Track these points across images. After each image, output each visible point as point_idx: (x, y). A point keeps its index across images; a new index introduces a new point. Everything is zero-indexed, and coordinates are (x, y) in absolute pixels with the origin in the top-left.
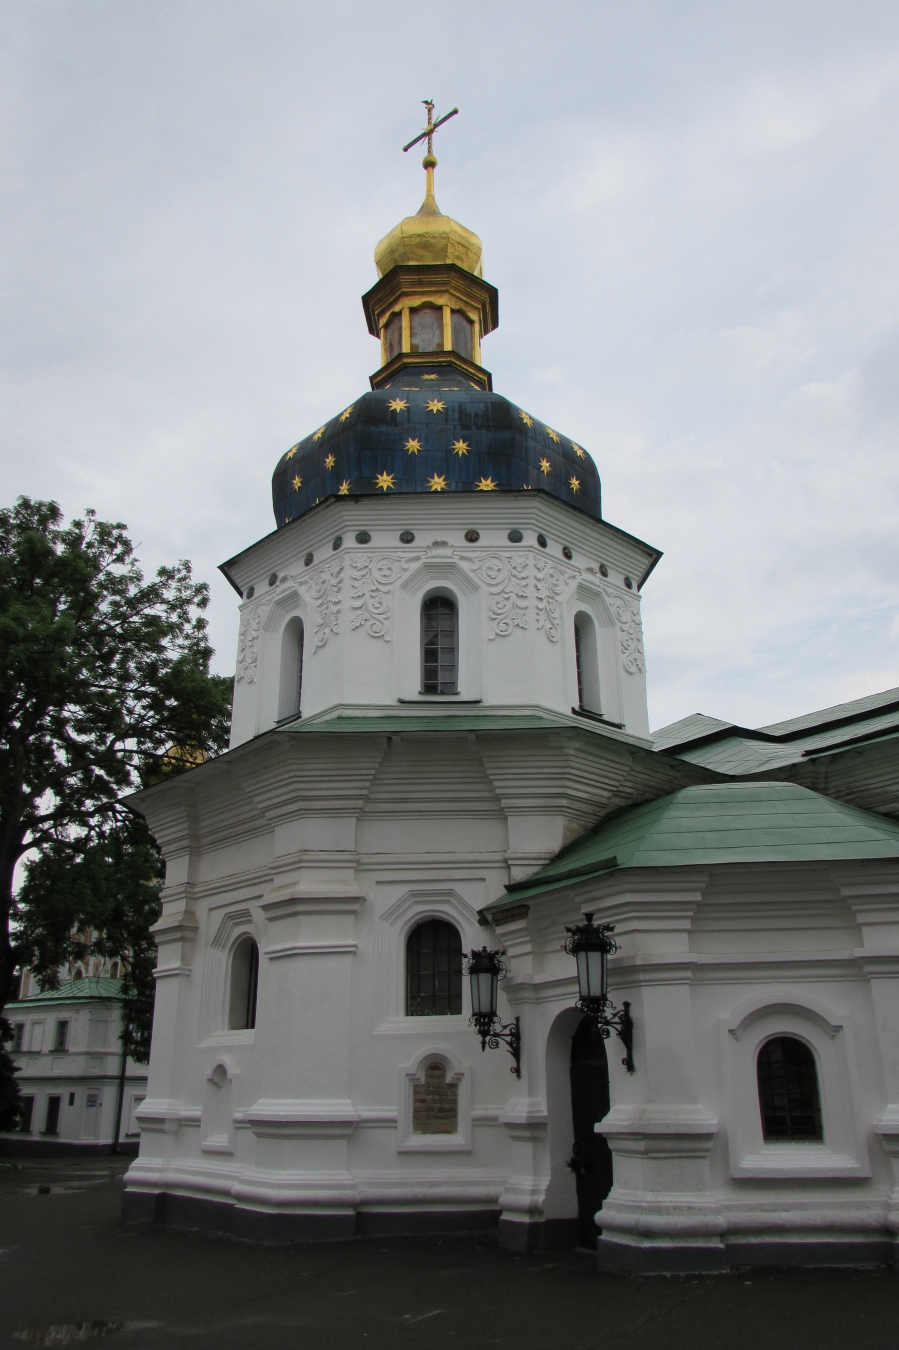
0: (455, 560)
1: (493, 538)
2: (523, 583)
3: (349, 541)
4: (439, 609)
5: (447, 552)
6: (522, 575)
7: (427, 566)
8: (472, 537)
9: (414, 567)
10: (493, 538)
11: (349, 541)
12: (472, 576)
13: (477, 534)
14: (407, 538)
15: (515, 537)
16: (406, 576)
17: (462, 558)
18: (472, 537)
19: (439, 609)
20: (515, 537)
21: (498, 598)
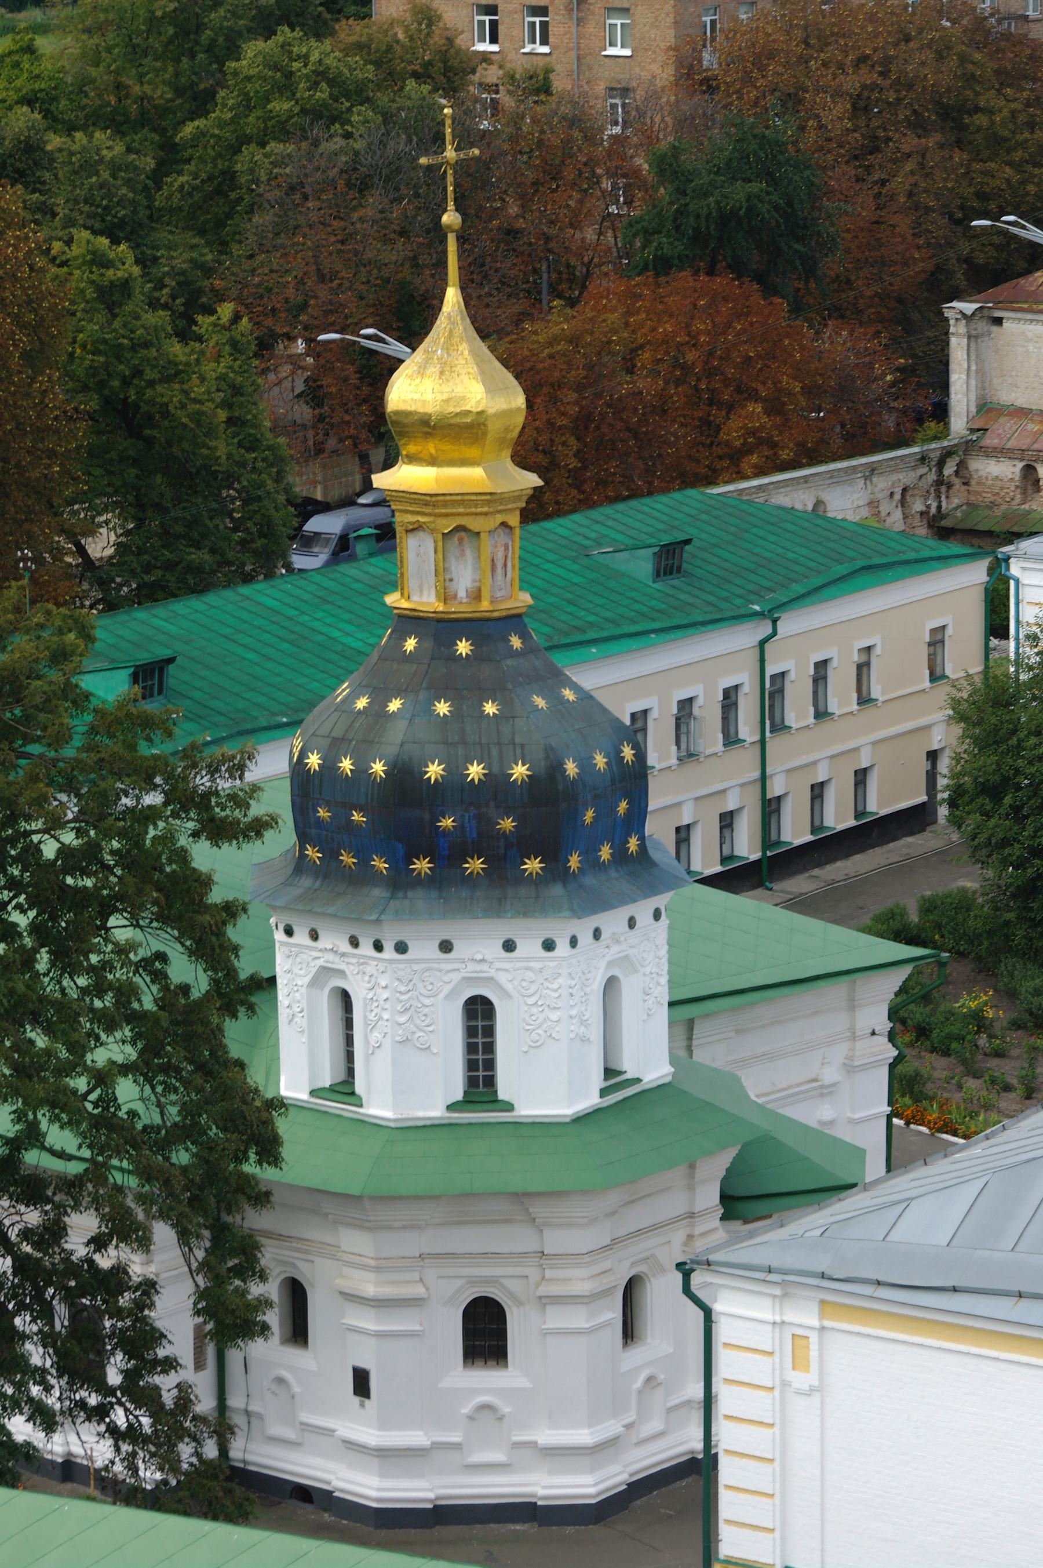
0: (492, 973)
1: (529, 947)
2: (556, 995)
4: (479, 1013)
5: (484, 967)
6: (555, 986)
7: (464, 978)
8: (509, 946)
9: (456, 977)
10: (529, 947)
12: (509, 987)
13: (513, 942)
14: (446, 947)
15: (549, 945)
16: (447, 989)
17: (498, 969)
18: (509, 946)
19: (479, 1013)
20: (549, 945)
21: (534, 1010)
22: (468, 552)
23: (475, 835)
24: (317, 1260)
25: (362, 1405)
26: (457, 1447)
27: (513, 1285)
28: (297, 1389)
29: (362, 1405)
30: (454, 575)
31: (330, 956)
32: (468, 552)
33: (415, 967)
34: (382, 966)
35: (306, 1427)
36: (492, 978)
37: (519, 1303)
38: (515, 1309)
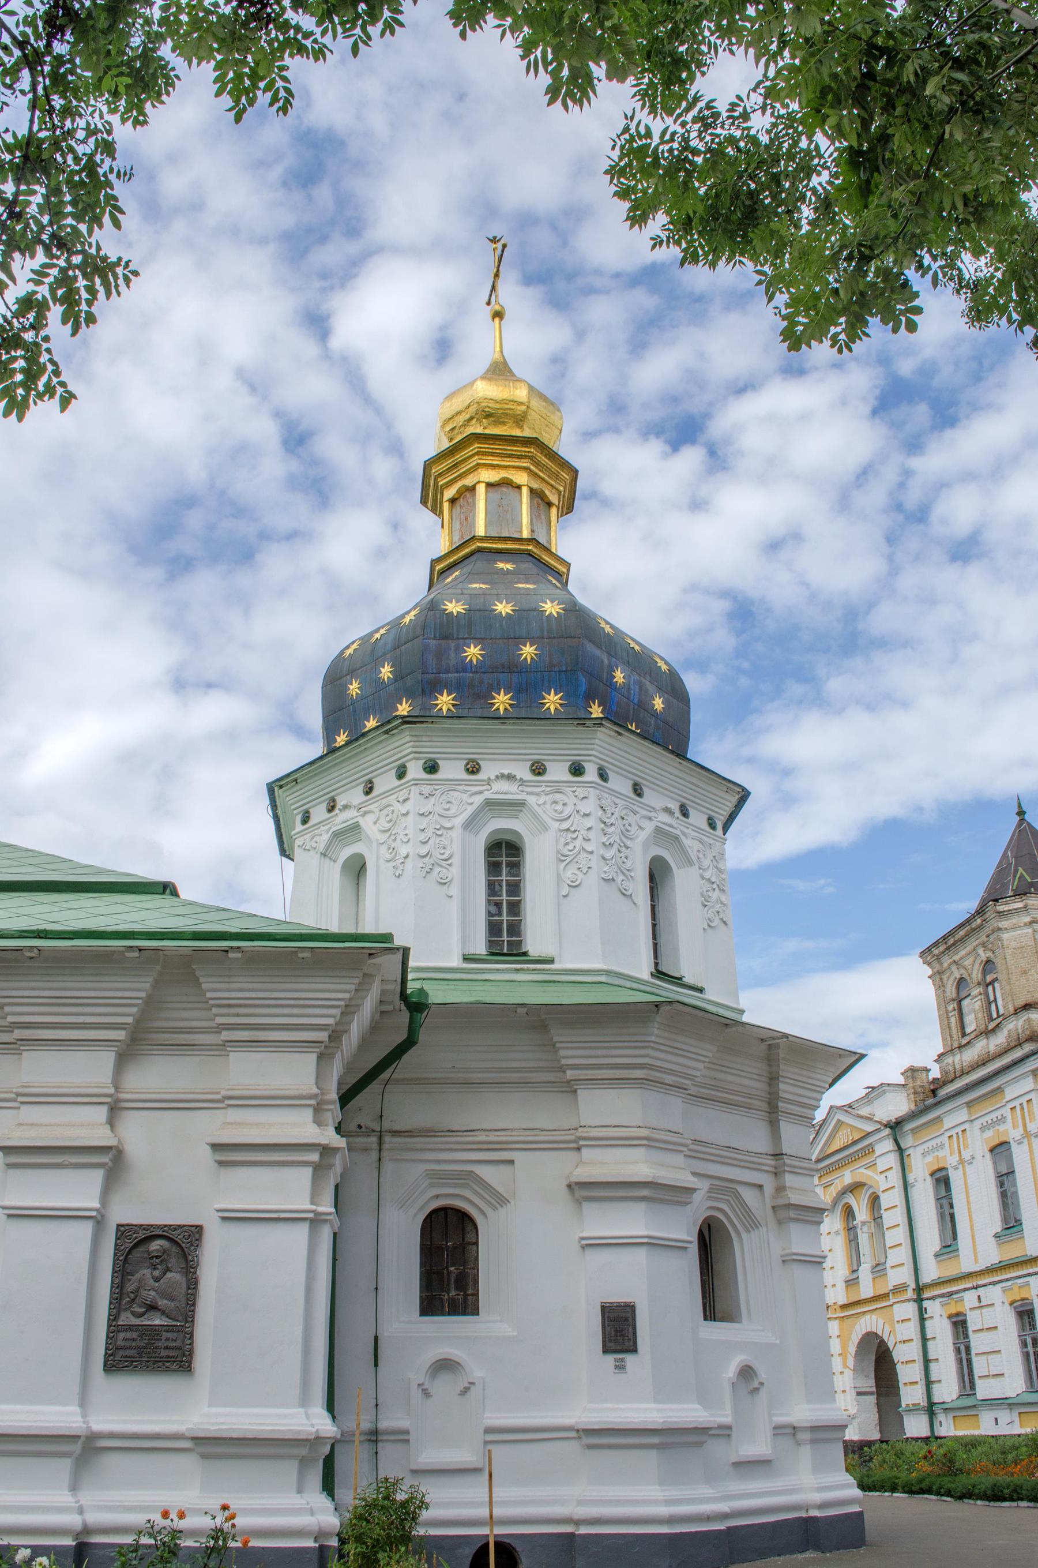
0: (678, 832)
3: (591, 774)
9: (649, 827)
11: (591, 774)
16: (643, 836)
21: (708, 886)
22: (543, 517)
23: (636, 701)
24: (518, 1156)
25: (620, 1367)
26: (724, 1432)
27: (749, 1196)
28: (477, 1373)
29: (620, 1367)
30: (535, 528)
31: (503, 786)
32: (543, 517)
33: (617, 801)
34: (581, 792)
35: (499, 1435)
36: (676, 838)
37: (752, 1223)
38: (744, 1235)
